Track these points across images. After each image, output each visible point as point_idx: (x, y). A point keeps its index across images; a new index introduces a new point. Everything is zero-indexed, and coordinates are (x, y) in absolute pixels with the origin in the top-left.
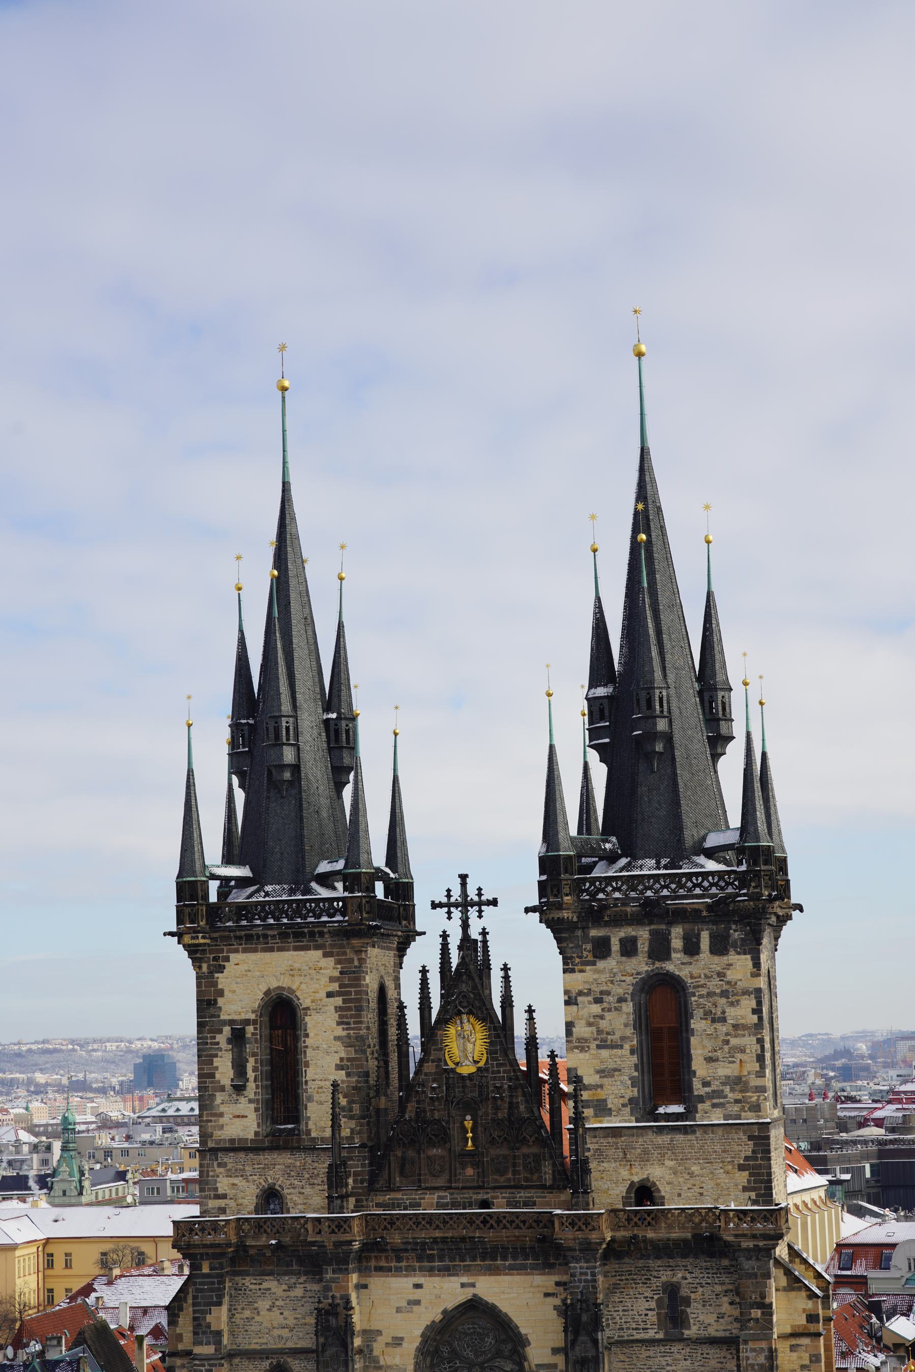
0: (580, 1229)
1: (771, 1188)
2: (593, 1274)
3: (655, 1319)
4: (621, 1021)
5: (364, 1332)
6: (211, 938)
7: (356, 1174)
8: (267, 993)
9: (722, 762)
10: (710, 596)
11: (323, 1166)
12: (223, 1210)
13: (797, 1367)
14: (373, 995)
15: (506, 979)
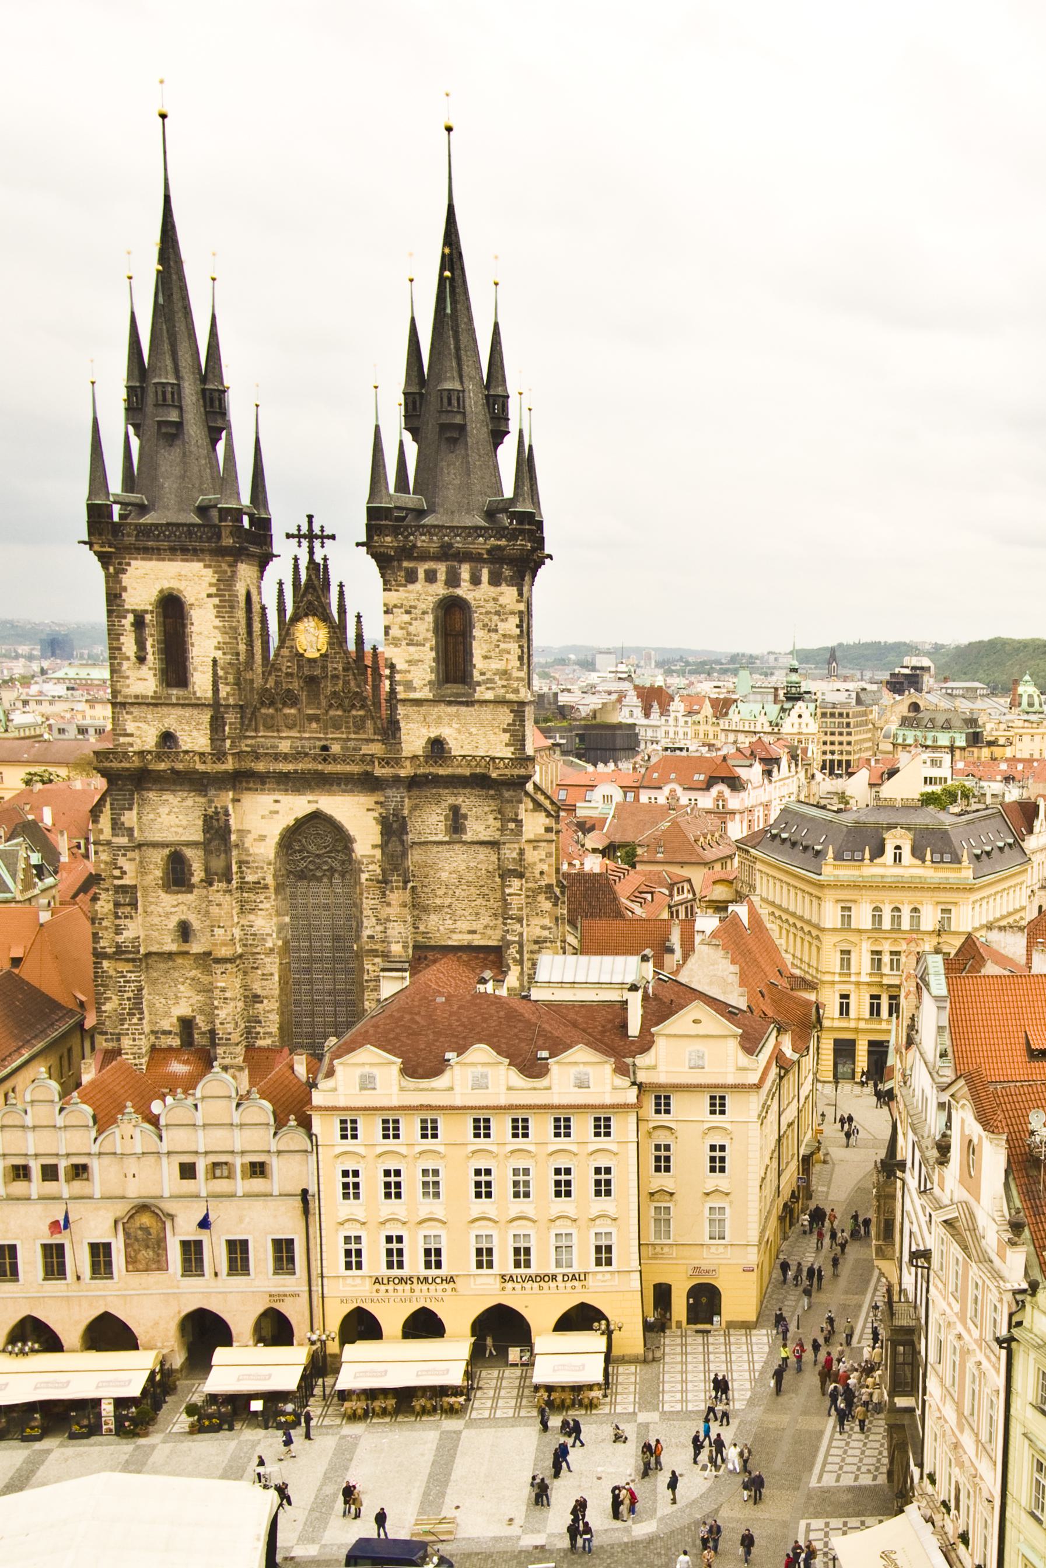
0: (393, 767)
1: (524, 745)
2: (401, 797)
3: (443, 828)
4: (425, 627)
5: (239, 831)
6: (115, 548)
7: (230, 724)
8: (161, 591)
9: (501, 449)
10: (496, 325)
11: (206, 716)
12: (131, 745)
13: (537, 860)
14: (242, 599)
15: (341, 594)
